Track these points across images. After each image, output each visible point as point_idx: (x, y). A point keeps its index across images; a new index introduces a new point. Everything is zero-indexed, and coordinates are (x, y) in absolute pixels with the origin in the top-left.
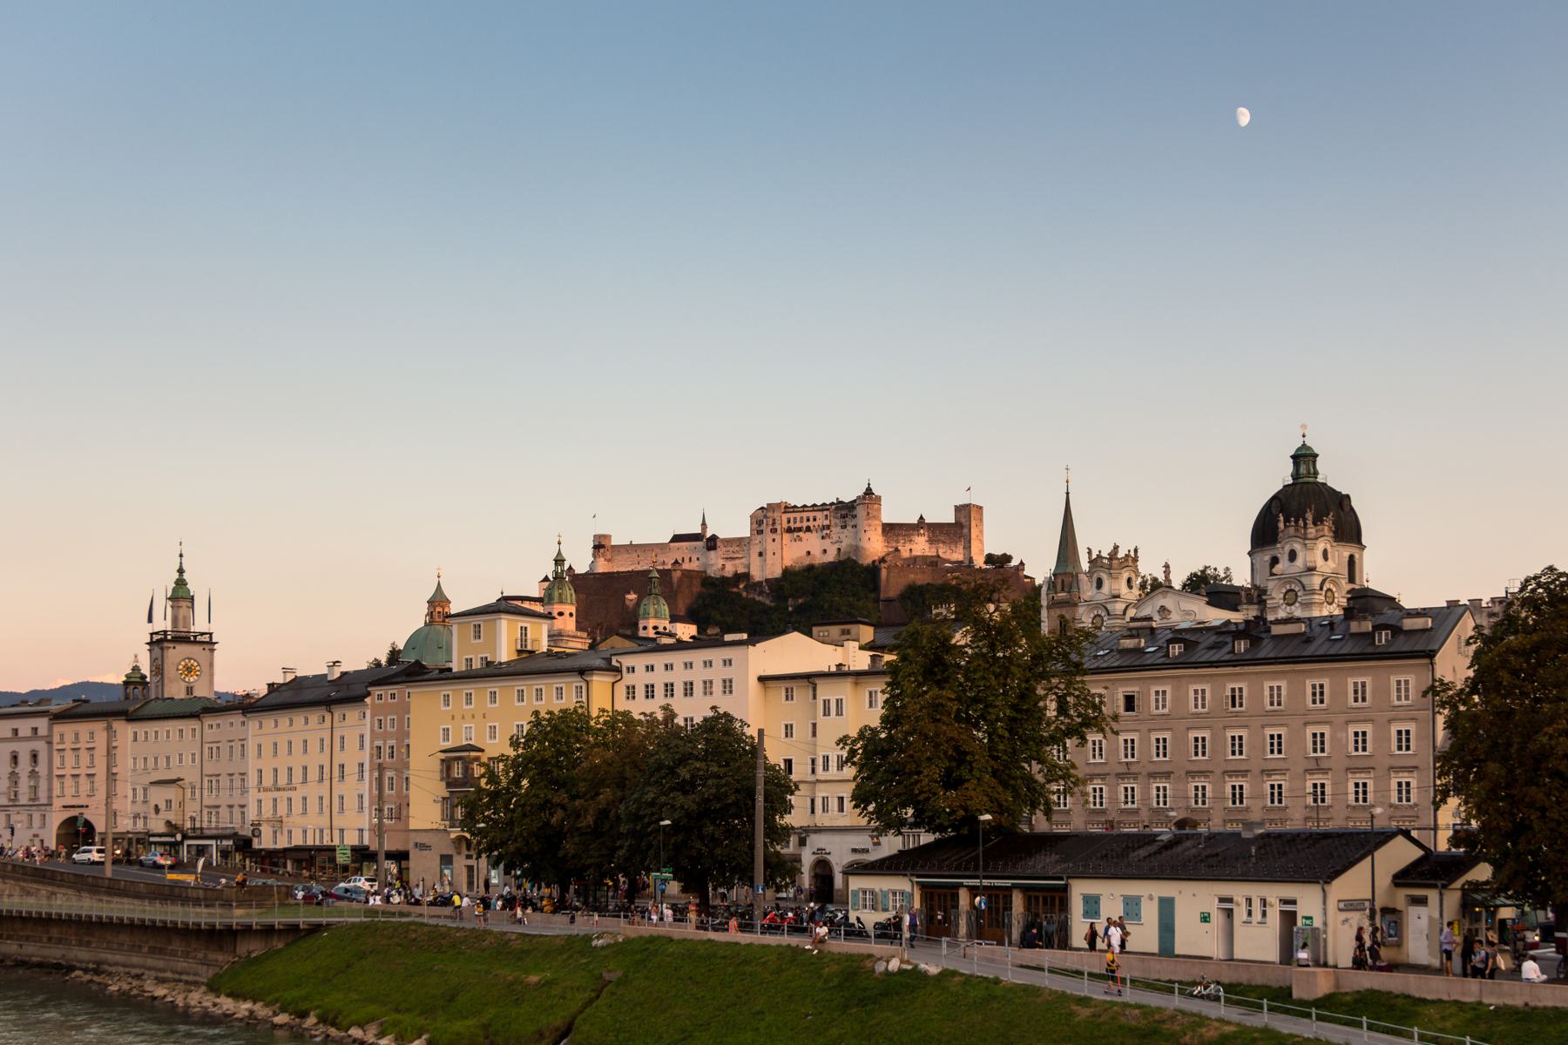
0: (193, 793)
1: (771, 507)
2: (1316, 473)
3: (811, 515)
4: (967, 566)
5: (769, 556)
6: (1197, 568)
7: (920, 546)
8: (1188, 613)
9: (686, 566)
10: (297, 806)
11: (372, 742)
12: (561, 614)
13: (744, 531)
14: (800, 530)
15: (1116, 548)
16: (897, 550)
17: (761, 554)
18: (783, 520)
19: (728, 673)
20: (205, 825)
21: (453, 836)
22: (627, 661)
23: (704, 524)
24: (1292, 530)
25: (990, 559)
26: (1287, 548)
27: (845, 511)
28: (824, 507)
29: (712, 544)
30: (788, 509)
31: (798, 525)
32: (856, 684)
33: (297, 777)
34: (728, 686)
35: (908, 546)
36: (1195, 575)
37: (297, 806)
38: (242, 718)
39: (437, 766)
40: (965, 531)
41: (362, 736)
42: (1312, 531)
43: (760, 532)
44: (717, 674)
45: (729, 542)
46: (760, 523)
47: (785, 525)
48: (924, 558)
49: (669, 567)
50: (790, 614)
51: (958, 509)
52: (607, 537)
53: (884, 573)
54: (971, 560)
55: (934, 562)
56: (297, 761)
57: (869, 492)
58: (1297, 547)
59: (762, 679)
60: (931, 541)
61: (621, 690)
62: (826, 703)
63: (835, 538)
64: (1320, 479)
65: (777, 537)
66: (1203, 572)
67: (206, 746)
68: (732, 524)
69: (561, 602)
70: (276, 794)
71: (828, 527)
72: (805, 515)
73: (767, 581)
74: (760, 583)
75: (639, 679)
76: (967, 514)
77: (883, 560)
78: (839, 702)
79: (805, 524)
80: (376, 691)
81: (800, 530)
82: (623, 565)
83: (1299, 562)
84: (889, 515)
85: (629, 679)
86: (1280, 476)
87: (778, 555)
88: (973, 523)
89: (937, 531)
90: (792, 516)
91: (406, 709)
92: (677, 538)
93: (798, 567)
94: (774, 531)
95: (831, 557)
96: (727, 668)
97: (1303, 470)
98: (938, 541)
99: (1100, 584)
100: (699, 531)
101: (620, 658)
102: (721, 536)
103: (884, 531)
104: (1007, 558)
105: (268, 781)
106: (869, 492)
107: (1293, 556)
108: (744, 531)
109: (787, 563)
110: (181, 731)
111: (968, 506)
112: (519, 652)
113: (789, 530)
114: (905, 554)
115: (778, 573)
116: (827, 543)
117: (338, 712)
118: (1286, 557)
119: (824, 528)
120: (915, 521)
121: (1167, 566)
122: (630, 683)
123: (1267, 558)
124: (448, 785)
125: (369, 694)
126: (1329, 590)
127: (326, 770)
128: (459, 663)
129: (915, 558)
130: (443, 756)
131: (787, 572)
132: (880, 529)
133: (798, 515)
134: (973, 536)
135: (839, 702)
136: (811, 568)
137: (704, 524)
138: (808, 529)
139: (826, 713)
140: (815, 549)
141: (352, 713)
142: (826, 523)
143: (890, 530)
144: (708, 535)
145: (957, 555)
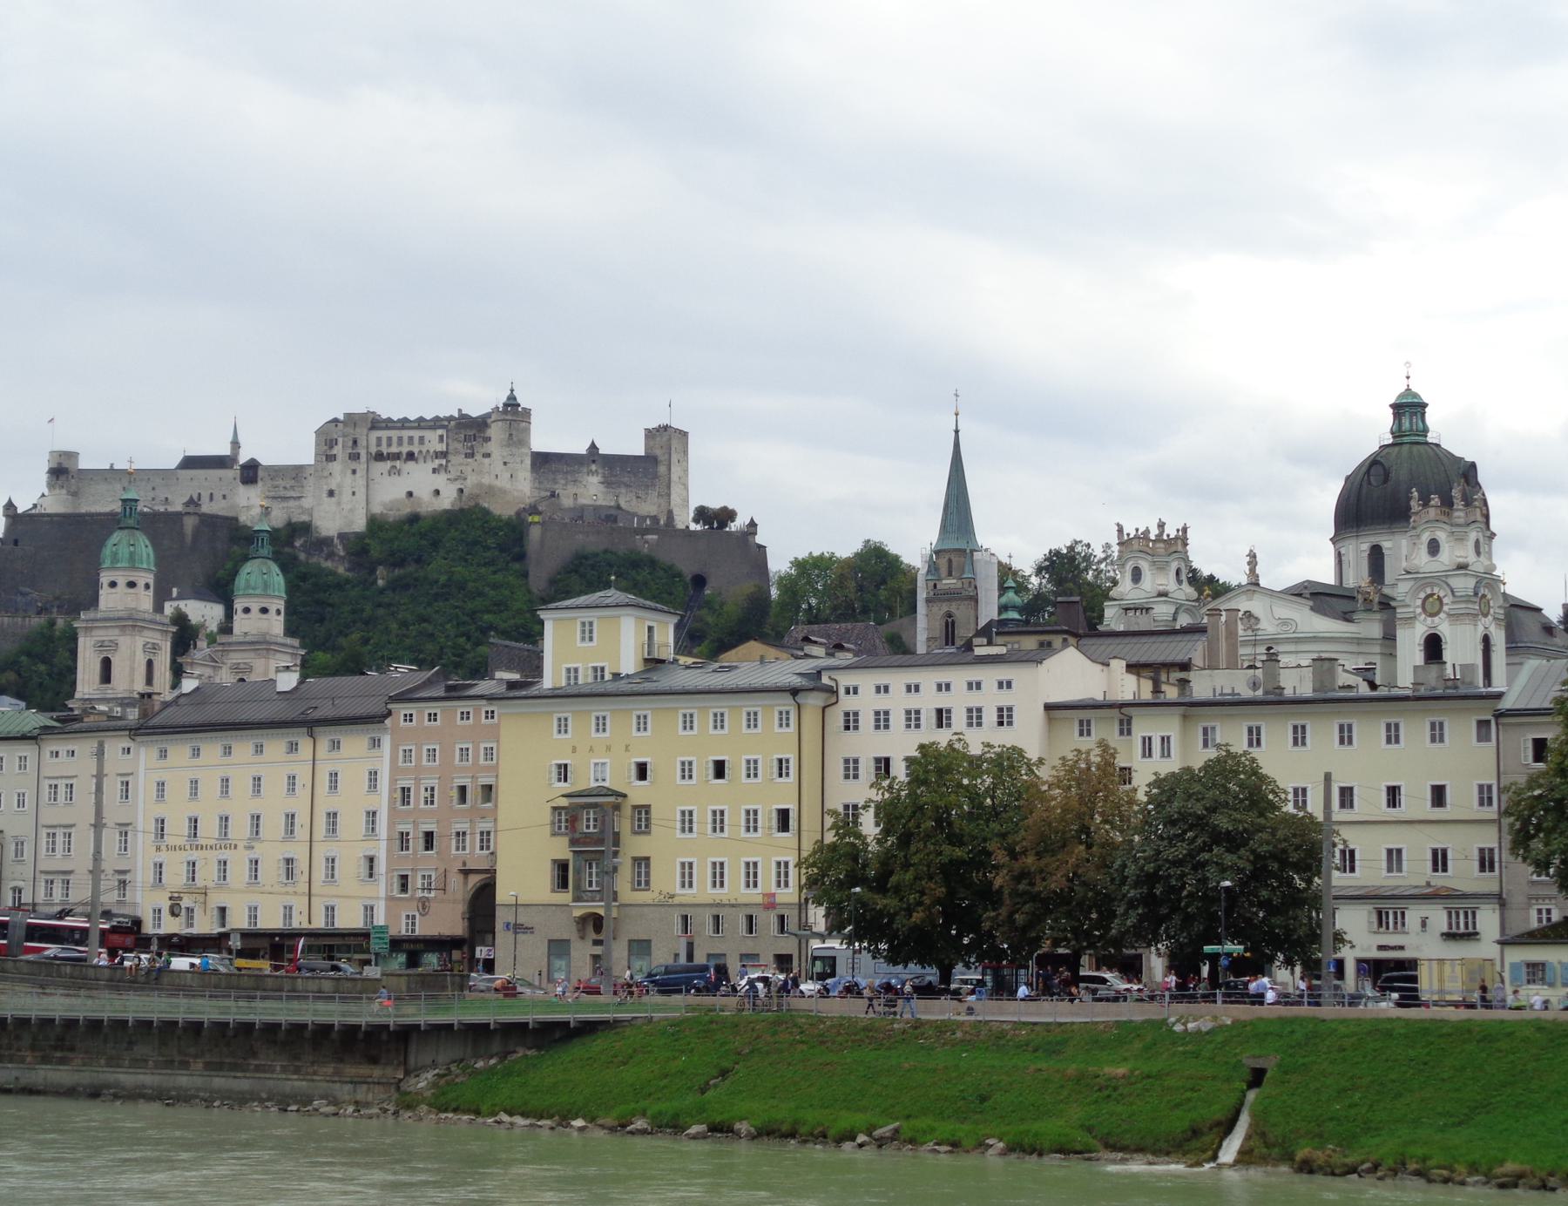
0: (19, 852)
1: (352, 420)
2: (1426, 430)
3: (416, 434)
4: (665, 527)
5: (346, 496)
6: (1062, 544)
7: (592, 490)
8: (1284, 622)
9: (206, 508)
10: (239, 871)
11: (393, 781)
12: (132, 585)
13: (303, 452)
14: (397, 456)
15: (1161, 525)
16: (553, 495)
17: (331, 493)
18: (371, 441)
19: (1005, 698)
20: (41, 896)
21: (578, 913)
22: (845, 680)
23: (236, 444)
24: (1432, 513)
25: (702, 514)
26: (1426, 537)
27: (469, 430)
28: (436, 423)
29: (251, 473)
30: (376, 423)
31: (394, 449)
32: (1185, 717)
33: (240, 829)
34: (1005, 717)
35: (571, 489)
36: (1058, 553)
37: (239, 871)
38: (126, 743)
39: (547, 816)
40: (662, 469)
41: (373, 775)
42: (1459, 514)
43: (331, 458)
44: (990, 699)
45: (277, 472)
46: (332, 443)
47: (373, 450)
48: (596, 508)
49: (178, 507)
50: (382, 591)
51: (650, 434)
52: (72, 456)
53: (535, 533)
54: (670, 514)
55: (610, 517)
56: (240, 807)
57: (512, 403)
58: (1441, 536)
59: (1049, 708)
60: (607, 483)
61: (836, 719)
62: (1147, 743)
63: (454, 473)
64: (1431, 438)
65: (361, 467)
66: (1071, 548)
67: (45, 784)
68: (284, 441)
69: (133, 568)
70: (195, 855)
71: (444, 455)
72: (406, 434)
73: (342, 536)
74: (327, 541)
75: (866, 703)
76: (666, 442)
77: (533, 510)
78: (1165, 740)
79: (405, 449)
80: (401, 710)
81: (397, 456)
82: (104, 502)
83: (1447, 556)
84: (543, 439)
85: (847, 703)
86: (1377, 430)
87: (361, 495)
88: (674, 458)
89: (615, 467)
90: (384, 434)
91: (494, 733)
92: (190, 463)
93: (393, 516)
94: (355, 457)
95: (447, 501)
96: (1005, 691)
97: (1406, 425)
98: (619, 484)
99: (1137, 575)
100: (224, 450)
101: (835, 675)
102: (264, 460)
103: (533, 465)
104: (727, 515)
105: (177, 829)
106: (512, 403)
107: (1434, 548)
108: (303, 452)
109: (377, 509)
110: (23, 759)
111: (666, 428)
112: (646, 660)
113: (380, 457)
114: (567, 502)
115: (360, 525)
116: (440, 481)
117: (324, 739)
118: (1424, 549)
119: (438, 455)
120: (581, 448)
121: (1253, 557)
122: (851, 708)
123: (1365, 547)
124: (573, 842)
125: (390, 713)
126: (1484, 596)
127: (302, 819)
128: (555, 672)
129: (583, 508)
130: (564, 802)
131: (375, 523)
132: (528, 461)
133: (394, 434)
134: (674, 477)
135: (1165, 740)
136: (414, 518)
137: (236, 444)
138: (411, 456)
139: (1147, 752)
140: (426, 487)
141: (354, 744)
142: (442, 447)
143: (543, 461)
144: (243, 458)
145: (648, 506)
